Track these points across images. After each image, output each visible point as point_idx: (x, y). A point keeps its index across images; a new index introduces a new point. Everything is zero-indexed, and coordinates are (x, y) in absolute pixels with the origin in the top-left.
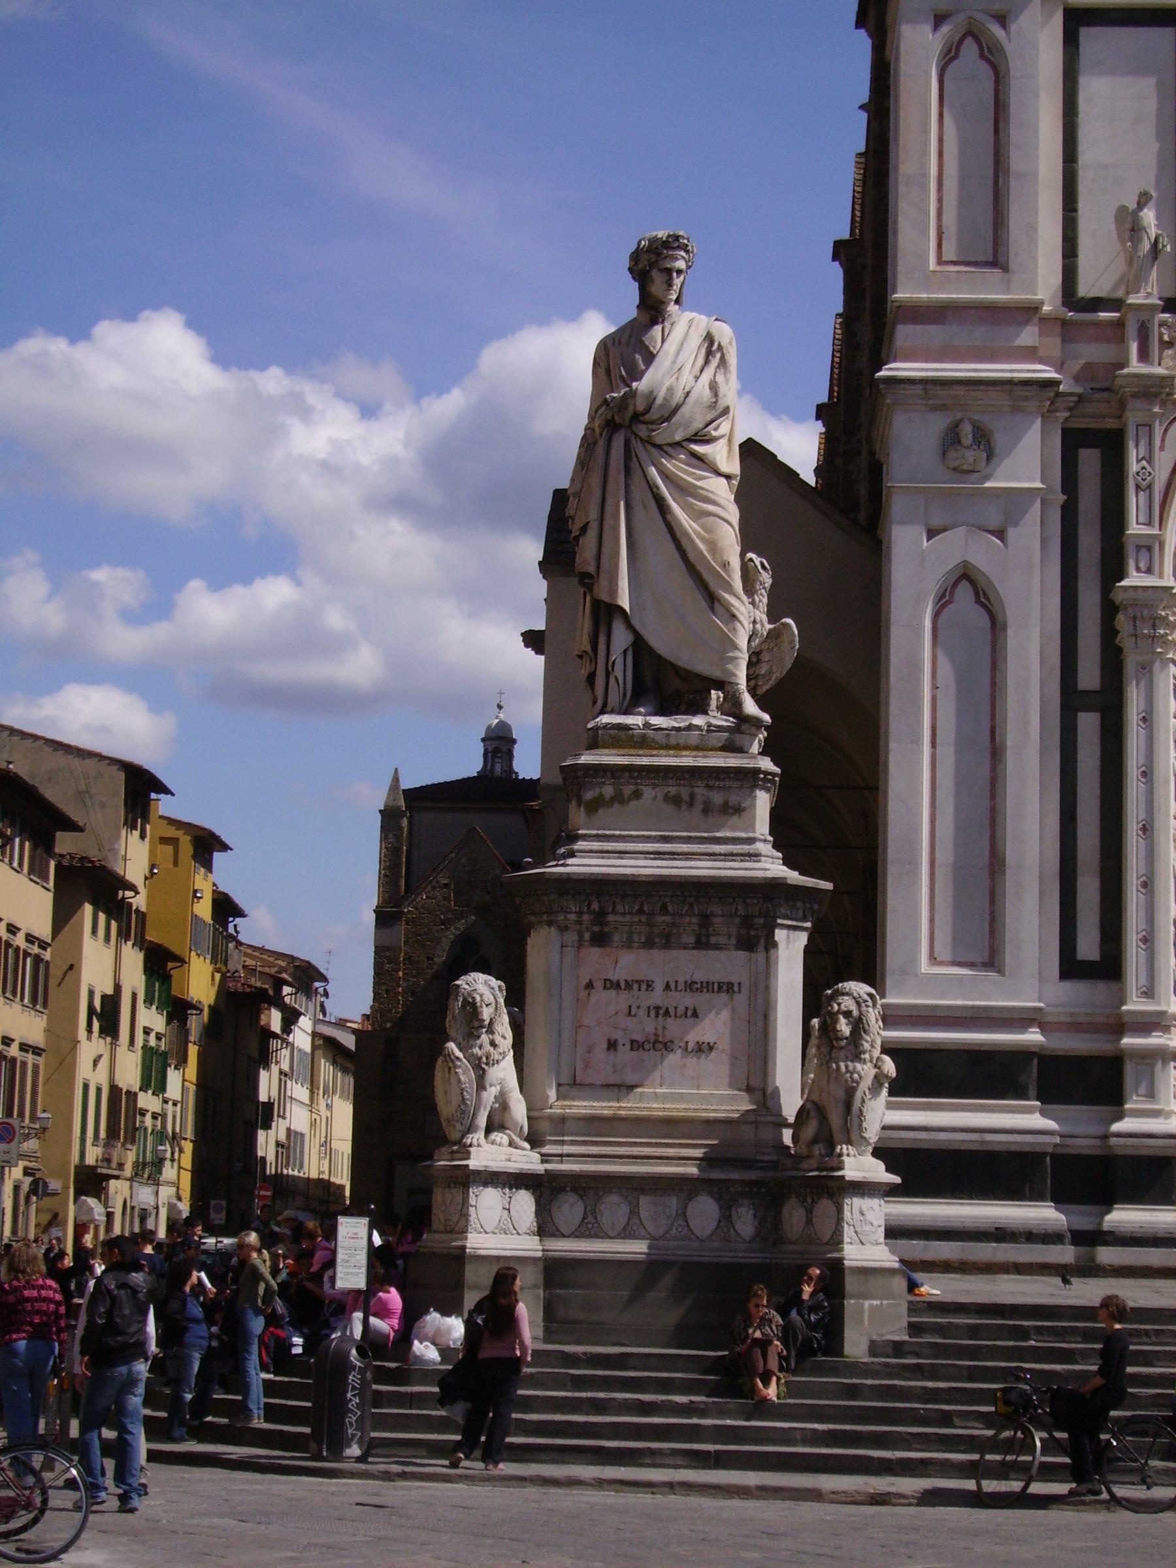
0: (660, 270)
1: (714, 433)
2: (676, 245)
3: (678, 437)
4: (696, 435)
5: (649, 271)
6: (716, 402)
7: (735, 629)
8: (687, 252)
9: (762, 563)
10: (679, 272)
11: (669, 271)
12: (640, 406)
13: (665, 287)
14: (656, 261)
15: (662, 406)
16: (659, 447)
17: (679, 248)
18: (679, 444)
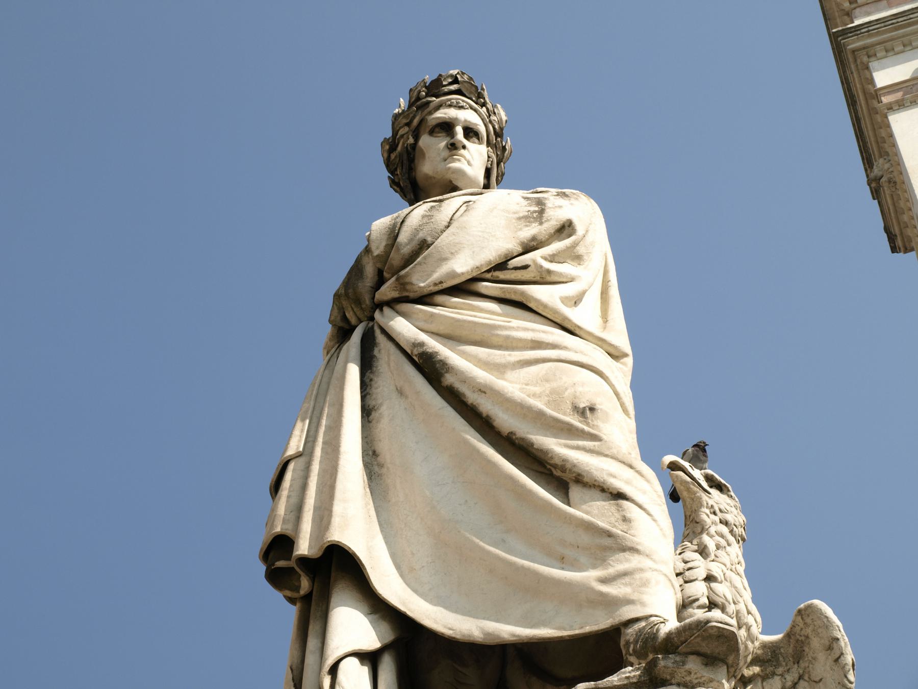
0: (432, 132)
1: (547, 265)
2: (454, 87)
3: (462, 265)
4: (502, 266)
5: (414, 146)
6: (542, 212)
7: (625, 520)
8: (483, 105)
9: (709, 478)
10: (470, 132)
11: (447, 127)
12: (378, 249)
13: (446, 153)
14: (422, 121)
15: (417, 230)
16: (426, 299)
17: (458, 92)
18: (464, 288)
